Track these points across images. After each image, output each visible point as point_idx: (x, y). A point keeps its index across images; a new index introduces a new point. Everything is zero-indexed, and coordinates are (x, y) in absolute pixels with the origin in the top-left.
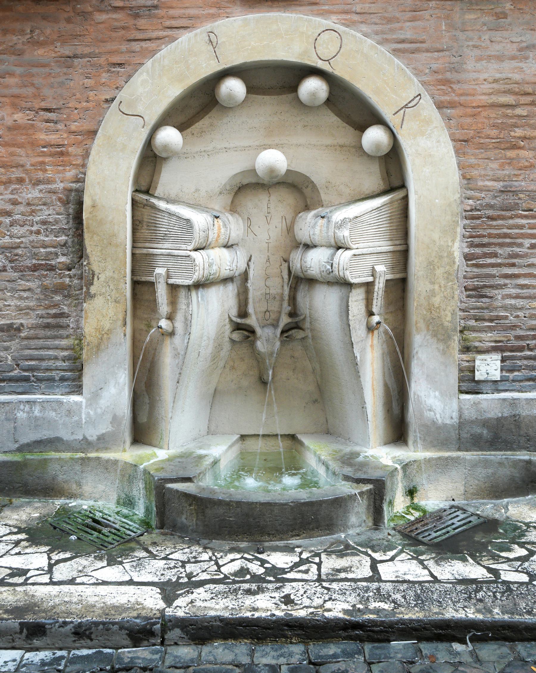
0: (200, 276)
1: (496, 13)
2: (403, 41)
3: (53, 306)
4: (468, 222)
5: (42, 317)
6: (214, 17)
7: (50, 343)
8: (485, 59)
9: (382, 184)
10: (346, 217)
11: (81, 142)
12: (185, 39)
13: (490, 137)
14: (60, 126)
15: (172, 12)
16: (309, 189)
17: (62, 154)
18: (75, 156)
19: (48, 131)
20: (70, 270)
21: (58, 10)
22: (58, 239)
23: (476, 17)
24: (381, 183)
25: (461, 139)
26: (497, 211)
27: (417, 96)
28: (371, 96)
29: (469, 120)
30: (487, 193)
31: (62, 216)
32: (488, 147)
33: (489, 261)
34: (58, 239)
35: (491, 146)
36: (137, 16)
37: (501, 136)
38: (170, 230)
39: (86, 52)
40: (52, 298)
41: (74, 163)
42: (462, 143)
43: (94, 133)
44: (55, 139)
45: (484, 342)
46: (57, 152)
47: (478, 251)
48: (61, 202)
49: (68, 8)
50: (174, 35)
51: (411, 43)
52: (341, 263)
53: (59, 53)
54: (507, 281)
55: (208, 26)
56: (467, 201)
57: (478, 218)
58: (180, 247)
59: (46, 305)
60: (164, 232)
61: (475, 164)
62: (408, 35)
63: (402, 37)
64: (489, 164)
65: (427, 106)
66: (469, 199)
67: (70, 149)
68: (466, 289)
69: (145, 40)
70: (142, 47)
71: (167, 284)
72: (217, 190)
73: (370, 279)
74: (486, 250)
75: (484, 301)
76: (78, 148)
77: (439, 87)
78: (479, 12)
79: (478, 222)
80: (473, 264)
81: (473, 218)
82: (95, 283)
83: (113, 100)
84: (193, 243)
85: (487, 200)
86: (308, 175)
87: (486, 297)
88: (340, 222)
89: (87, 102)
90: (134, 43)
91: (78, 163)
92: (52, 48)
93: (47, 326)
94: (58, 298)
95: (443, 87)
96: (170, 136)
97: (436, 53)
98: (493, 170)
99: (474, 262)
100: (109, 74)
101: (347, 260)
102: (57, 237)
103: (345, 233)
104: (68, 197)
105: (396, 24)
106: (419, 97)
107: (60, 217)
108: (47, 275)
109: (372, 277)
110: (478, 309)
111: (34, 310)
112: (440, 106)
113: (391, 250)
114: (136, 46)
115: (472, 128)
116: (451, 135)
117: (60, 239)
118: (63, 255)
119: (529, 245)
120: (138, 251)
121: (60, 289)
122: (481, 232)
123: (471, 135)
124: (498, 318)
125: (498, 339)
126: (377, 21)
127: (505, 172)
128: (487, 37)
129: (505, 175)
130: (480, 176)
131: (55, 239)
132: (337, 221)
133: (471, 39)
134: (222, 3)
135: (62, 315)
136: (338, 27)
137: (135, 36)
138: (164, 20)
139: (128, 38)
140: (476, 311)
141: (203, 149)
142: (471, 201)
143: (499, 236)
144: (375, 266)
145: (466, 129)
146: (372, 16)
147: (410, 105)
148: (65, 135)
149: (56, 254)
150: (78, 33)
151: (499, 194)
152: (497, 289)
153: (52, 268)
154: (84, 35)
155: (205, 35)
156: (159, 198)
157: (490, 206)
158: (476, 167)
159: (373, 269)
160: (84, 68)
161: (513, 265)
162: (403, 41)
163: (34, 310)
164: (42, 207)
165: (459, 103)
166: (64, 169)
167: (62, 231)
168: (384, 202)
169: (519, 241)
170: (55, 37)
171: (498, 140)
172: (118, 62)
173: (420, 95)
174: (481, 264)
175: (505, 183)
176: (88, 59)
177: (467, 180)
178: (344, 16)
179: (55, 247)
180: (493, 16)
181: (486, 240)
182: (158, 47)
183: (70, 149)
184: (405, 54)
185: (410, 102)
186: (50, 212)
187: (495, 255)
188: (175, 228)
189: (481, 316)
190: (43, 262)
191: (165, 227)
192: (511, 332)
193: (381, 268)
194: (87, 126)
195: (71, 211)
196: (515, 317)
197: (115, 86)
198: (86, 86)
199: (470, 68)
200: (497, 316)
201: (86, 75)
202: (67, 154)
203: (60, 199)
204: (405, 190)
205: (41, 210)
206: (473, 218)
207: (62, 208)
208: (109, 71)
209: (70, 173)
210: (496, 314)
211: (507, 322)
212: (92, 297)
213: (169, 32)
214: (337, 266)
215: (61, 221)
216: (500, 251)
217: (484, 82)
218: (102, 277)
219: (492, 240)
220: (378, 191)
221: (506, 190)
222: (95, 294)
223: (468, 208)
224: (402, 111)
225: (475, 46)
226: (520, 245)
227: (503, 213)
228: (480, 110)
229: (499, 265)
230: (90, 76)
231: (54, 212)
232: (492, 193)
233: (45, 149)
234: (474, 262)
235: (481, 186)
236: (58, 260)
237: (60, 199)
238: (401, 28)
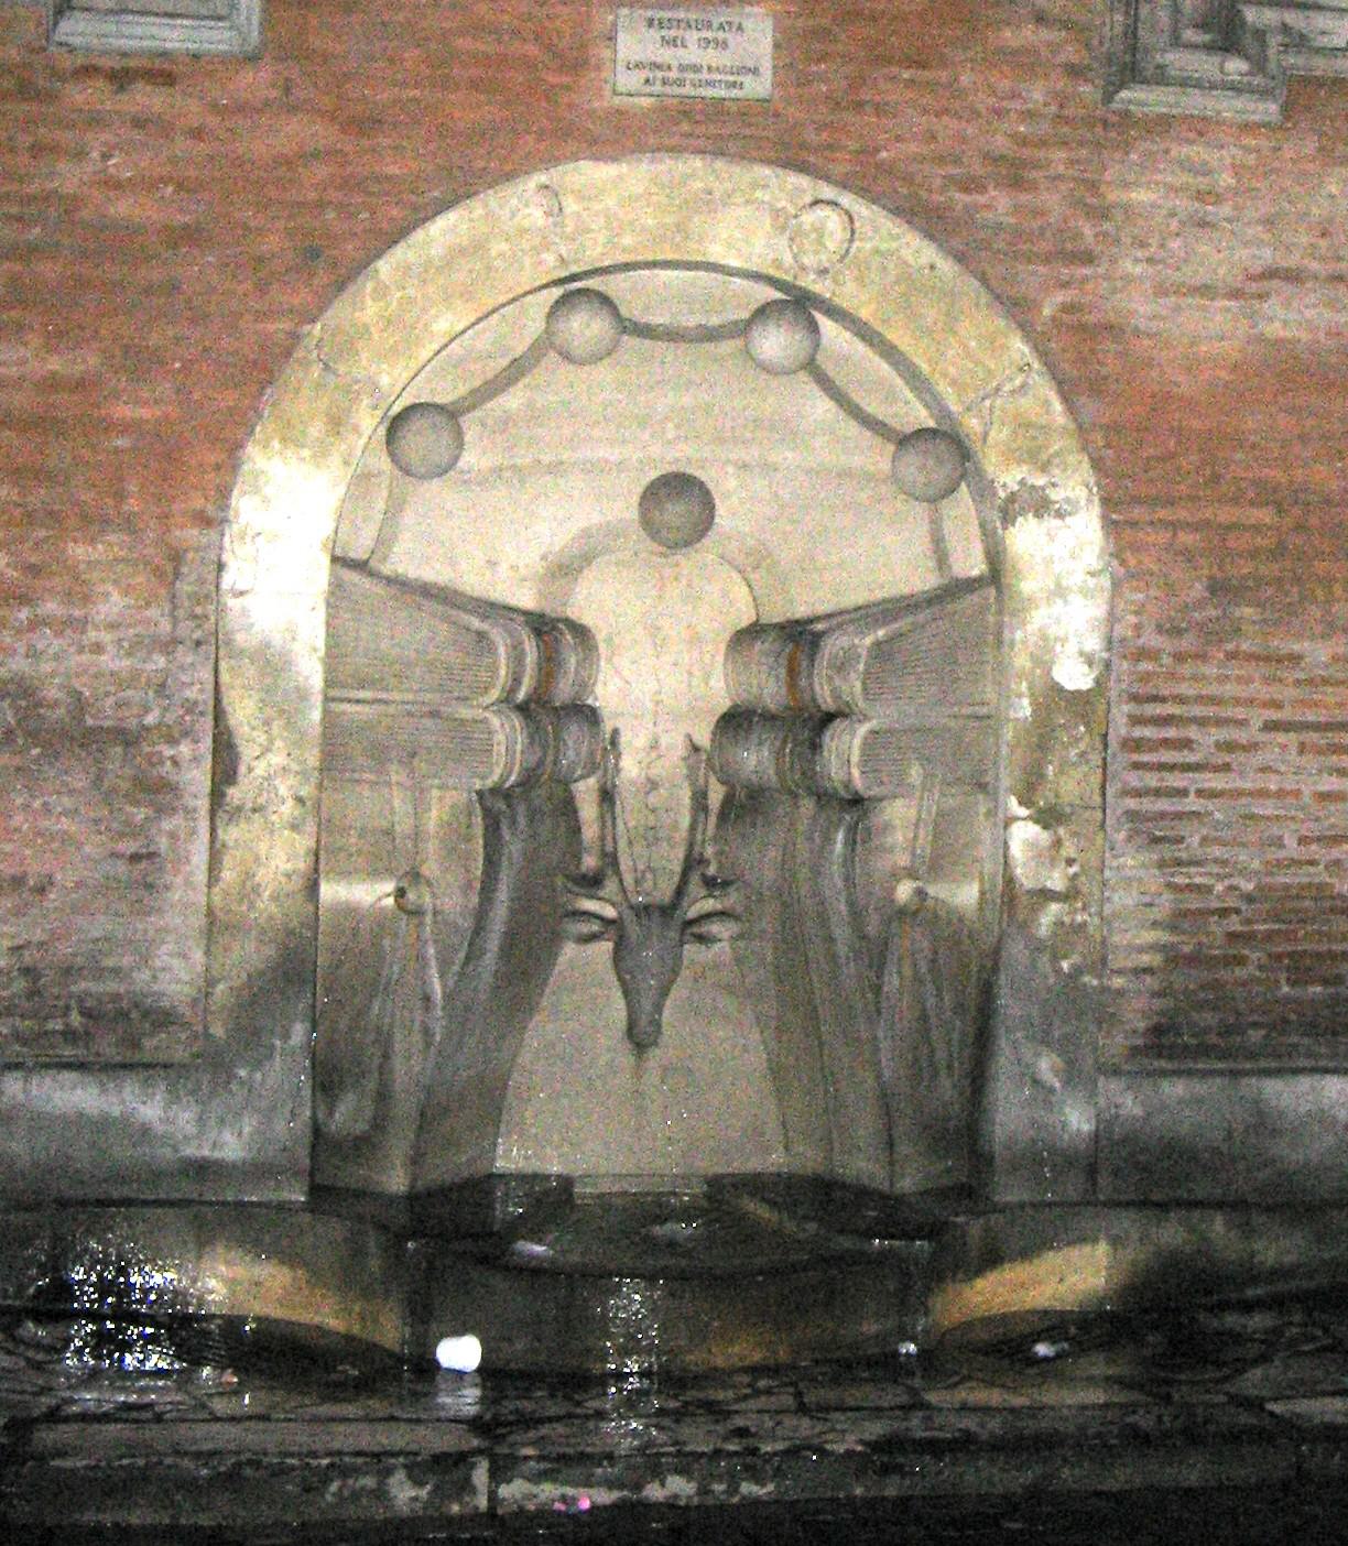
47: (1148, 732)
119: (1260, 724)
161: (1226, 767)
169: (1240, 713)
187: (1187, 744)
218: (260, 769)
226: (1242, 723)
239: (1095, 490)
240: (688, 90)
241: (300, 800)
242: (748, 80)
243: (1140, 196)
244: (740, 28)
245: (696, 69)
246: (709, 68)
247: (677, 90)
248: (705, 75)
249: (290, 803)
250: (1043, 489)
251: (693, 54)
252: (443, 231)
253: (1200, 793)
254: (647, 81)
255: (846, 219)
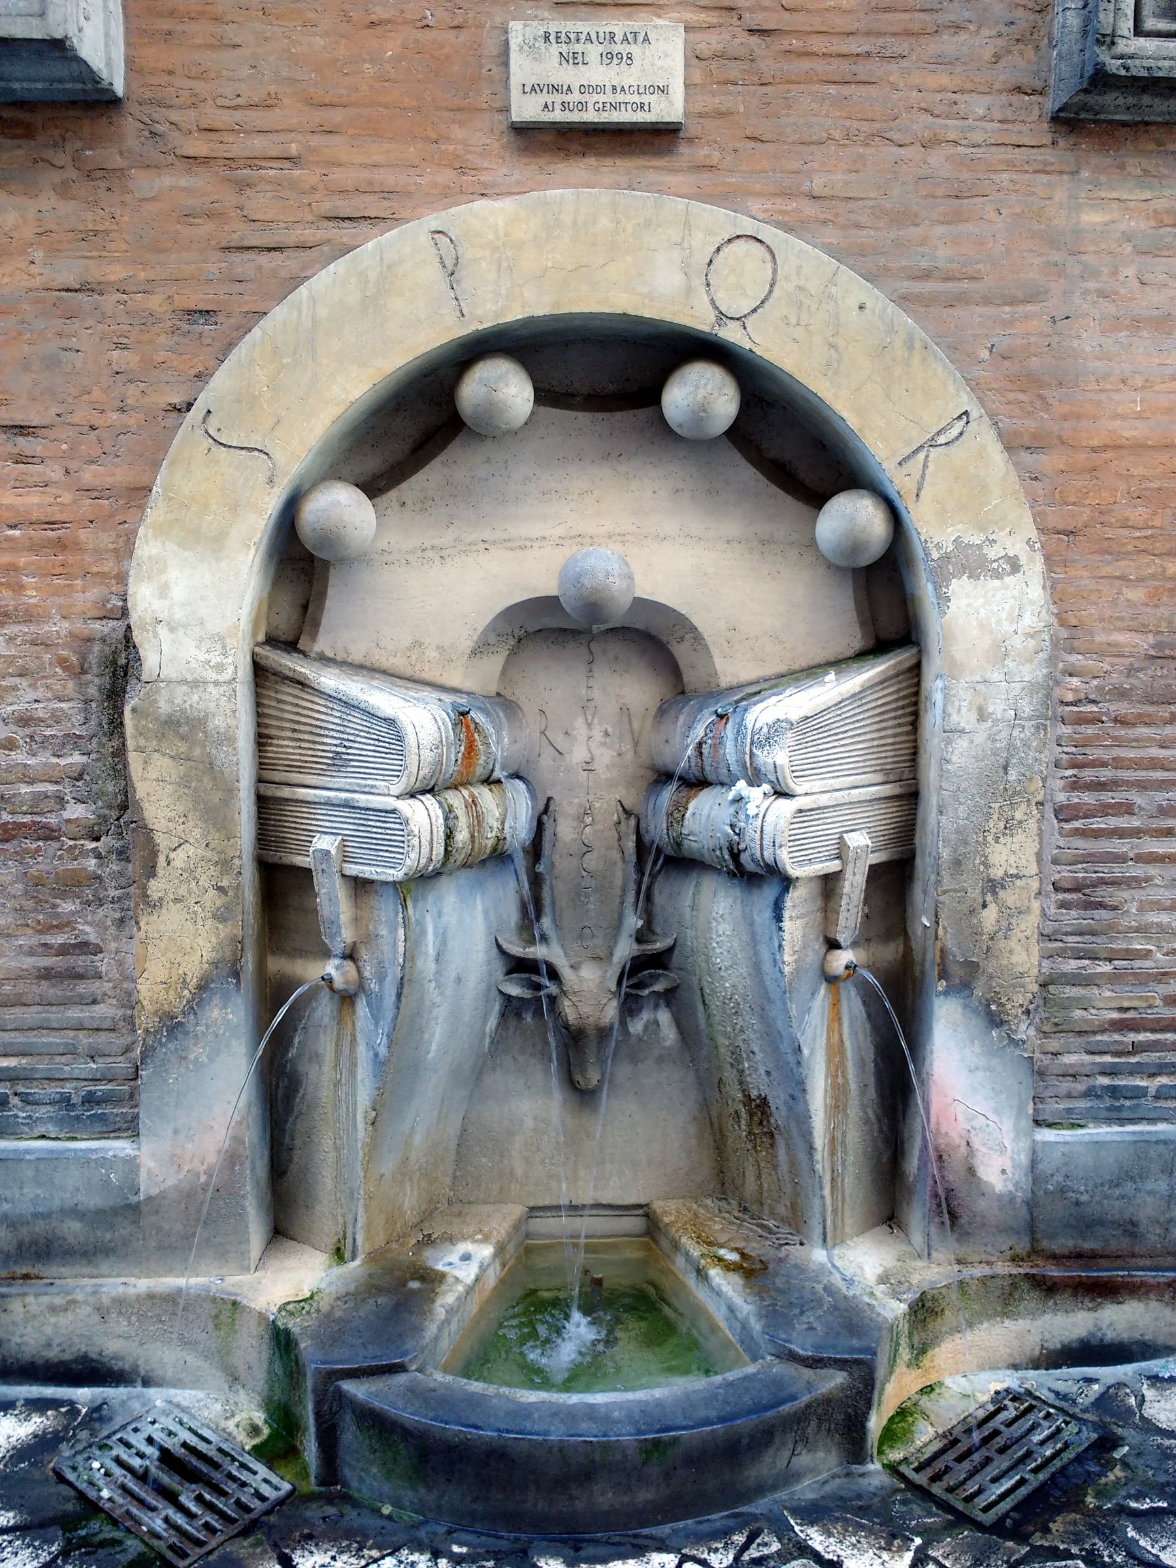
0: (423, 861)
1: (1155, 211)
2: (926, 275)
3: (57, 927)
4: (1067, 730)
5: (31, 953)
6: (448, 196)
7: (54, 1015)
8: (1127, 328)
9: (859, 636)
10: (782, 717)
11: (112, 516)
12: (375, 248)
13: (1130, 524)
14: (53, 472)
15: (337, 176)
16: (686, 644)
17: (61, 545)
18: (96, 551)
19: (21, 484)
20: (97, 839)
21: (35, 161)
22: (63, 762)
23: (1107, 218)
24: (857, 631)
25: (1061, 527)
26: (1138, 705)
27: (960, 417)
28: (844, 414)
29: (1080, 482)
30: (1115, 660)
31: (70, 704)
32: (1123, 550)
33: (1114, 822)
34: (63, 762)
35: (1130, 548)
36: (243, 186)
37: (1157, 522)
38: (346, 744)
39: (112, 278)
40: (55, 906)
41: (95, 569)
42: (1061, 541)
43: (140, 493)
44: (39, 506)
45: (1093, 1011)
46: (49, 540)
48: (65, 669)
49: (61, 159)
50: (345, 240)
51: (947, 279)
52: (768, 829)
53: (44, 279)
54: (1153, 870)
55: (433, 221)
56: (1068, 679)
57: (1096, 720)
58: (372, 787)
59: (39, 922)
60: (333, 748)
61: (1091, 591)
62: (943, 256)
63: (925, 264)
64: (1125, 590)
65: (984, 441)
66: (1071, 675)
67: (83, 535)
68: (1057, 888)
69: (270, 249)
70: (260, 268)
71: (343, 875)
72: (467, 645)
73: (835, 866)
74: (1107, 797)
75: (1097, 917)
76: (104, 530)
77: (1011, 396)
78: (1115, 205)
79: (1090, 730)
80: (1077, 829)
81: (1081, 720)
82: (160, 872)
83: (189, 406)
84: (404, 779)
85: (1116, 678)
86: (683, 612)
87: (1101, 906)
88: (765, 730)
89: (122, 410)
90: (236, 257)
91: (106, 569)
92: (23, 265)
93: (46, 974)
94: (67, 907)
95: (1021, 396)
96: (342, 508)
97: (1007, 309)
98: (1131, 604)
99: (1077, 824)
100: (176, 338)
101: (783, 823)
102: (59, 756)
103: (778, 756)
104: (83, 658)
105: (912, 229)
106: (965, 418)
107: (64, 705)
108: (38, 850)
109: (837, 862)
110: (1081, 934)
111: (9, 935)
112: (1011, 444)
113: (883, 795)
114: (244, 264)
115: (1087, 502)
116: (1038, 517)
117: (69, 760)
118: (79, 801)
120: (271, 791)
121: (71, 885)
122: (1094, 753)
123: (1085, 518)
124: (1130, 955)
125: (1126, 1004)
126: (863, 219)
127: (1159, 612)
128: (1130, 271)
129: (1161, 619)
130: (1102, 620)
131: (55, 760)
132: (758, 726)
133: (1095, 274)
134: (470, 157)
135: (84, 947)
136: (768, 233)
137: (242, 239)
138: (317, 197)
139: (224, 244)
140: (1078, 939)
141: (427, 544)
142: (1075, 679)
143: (1138, 764)
144: (845, 835)
145: (1074, 504)
146: (851, 205)
147: (942, 439)
148: (67, 498)
149: (61, 800)
150: (91, 227)
151: (1147, 663)
152: (1129, 887)
153: (50, 834)
154: (107, 232)
155: (424, 239)
156: (324, 660)
157: (1122, 694)
158: (1093, 597)
159: (842, 844)
160: (109, 321)
162: (926, 275)
163: (9, 935)
164: (17, 680)
165: (1060, 438)
166: (69, 585)
167: (73, 741)
168: (868, 680)
170: (28, 233)
171: (1150, 532)
172: (199, 308)
173: (966, 413)
174: (1093, 830)
175: (1159, 638)
176: (120, 296)
177: (1068, 631)
178: (780, 204)
179: (57, 783)
180: (1148, 219)
181: (1106, 774)
182: (303, 268)
183: (83, 535)
184: (931, 309)
185: (938, 433)
186: (39, 694)
187: (1128, 809)
188: (358, 739)
189: (1092, 951)
190: (27, 819)
191: (335, 734)
192: (1156, 989)
193: (858, 840)
194: (120, 475)
195: (93, 691)
196: (1167, 954)
197: (193, 372)
198: (115, 368)
199: (1088, 349)
200: (1127, 950)
201: (116, 340)
202: (78, 547)
203: (62, 662)
204: (914, 650)
205: (15, 688)
206: (1081, 720)
207: (71, 685)
208: (175, 330)
209: (87, 596)
210: (1124, 946)
211: (1148, 964)
212: (154, 906)
213: (331, 231)
214: (758, 836)
215: (68, 718)
216: (1137, 798)
217: (1121, 386)
218: (179, 858)
219: (1123, 774)
220: (851, 653)
221: (1160, 654)
222: (161, 899)
223: (1070, 697)
224: (921, 456)
225: (1102, 294)
227: (1151, 709)
228: (1109, 455)
229: (1136, 833)
230: (125, 341)
231: (49, 695)
232: (1127, 661)
233: (17, 533)
234: (1077, 824)
235: (1101, 644)
236: (66, 815)
237: (62, 662)
238: (924, 241)
239: (1037, 546)
240: (590, 116)
241: (220, 889)
242: (653, 99)
243: (1091, 218)
244: (646, 39)
245: (599, 89)
246: (614, 88)
247: (575, 117)
248: (609, 97)
249: (212, 892)
250: (980, 547)
251: (596, 73)
252: (328, 283)
253: (1140, 859)
254: (546, 106)
255: (768, 257)
